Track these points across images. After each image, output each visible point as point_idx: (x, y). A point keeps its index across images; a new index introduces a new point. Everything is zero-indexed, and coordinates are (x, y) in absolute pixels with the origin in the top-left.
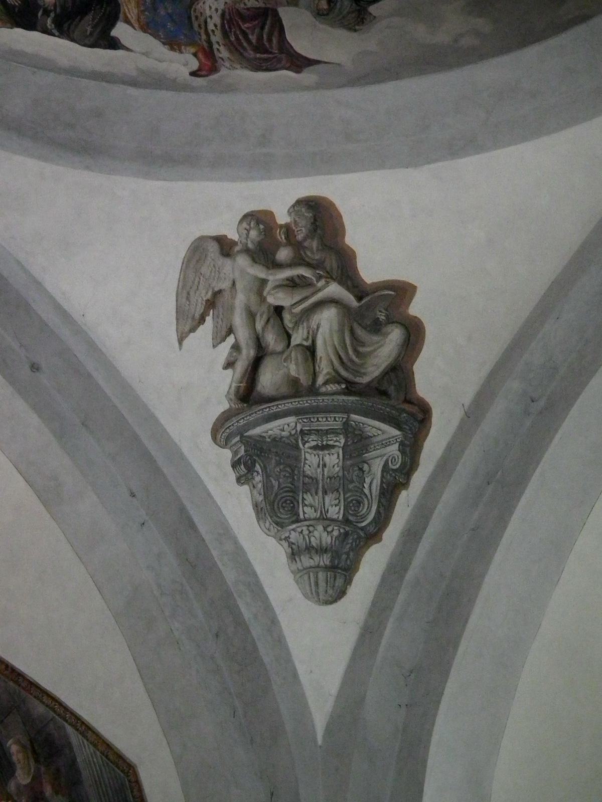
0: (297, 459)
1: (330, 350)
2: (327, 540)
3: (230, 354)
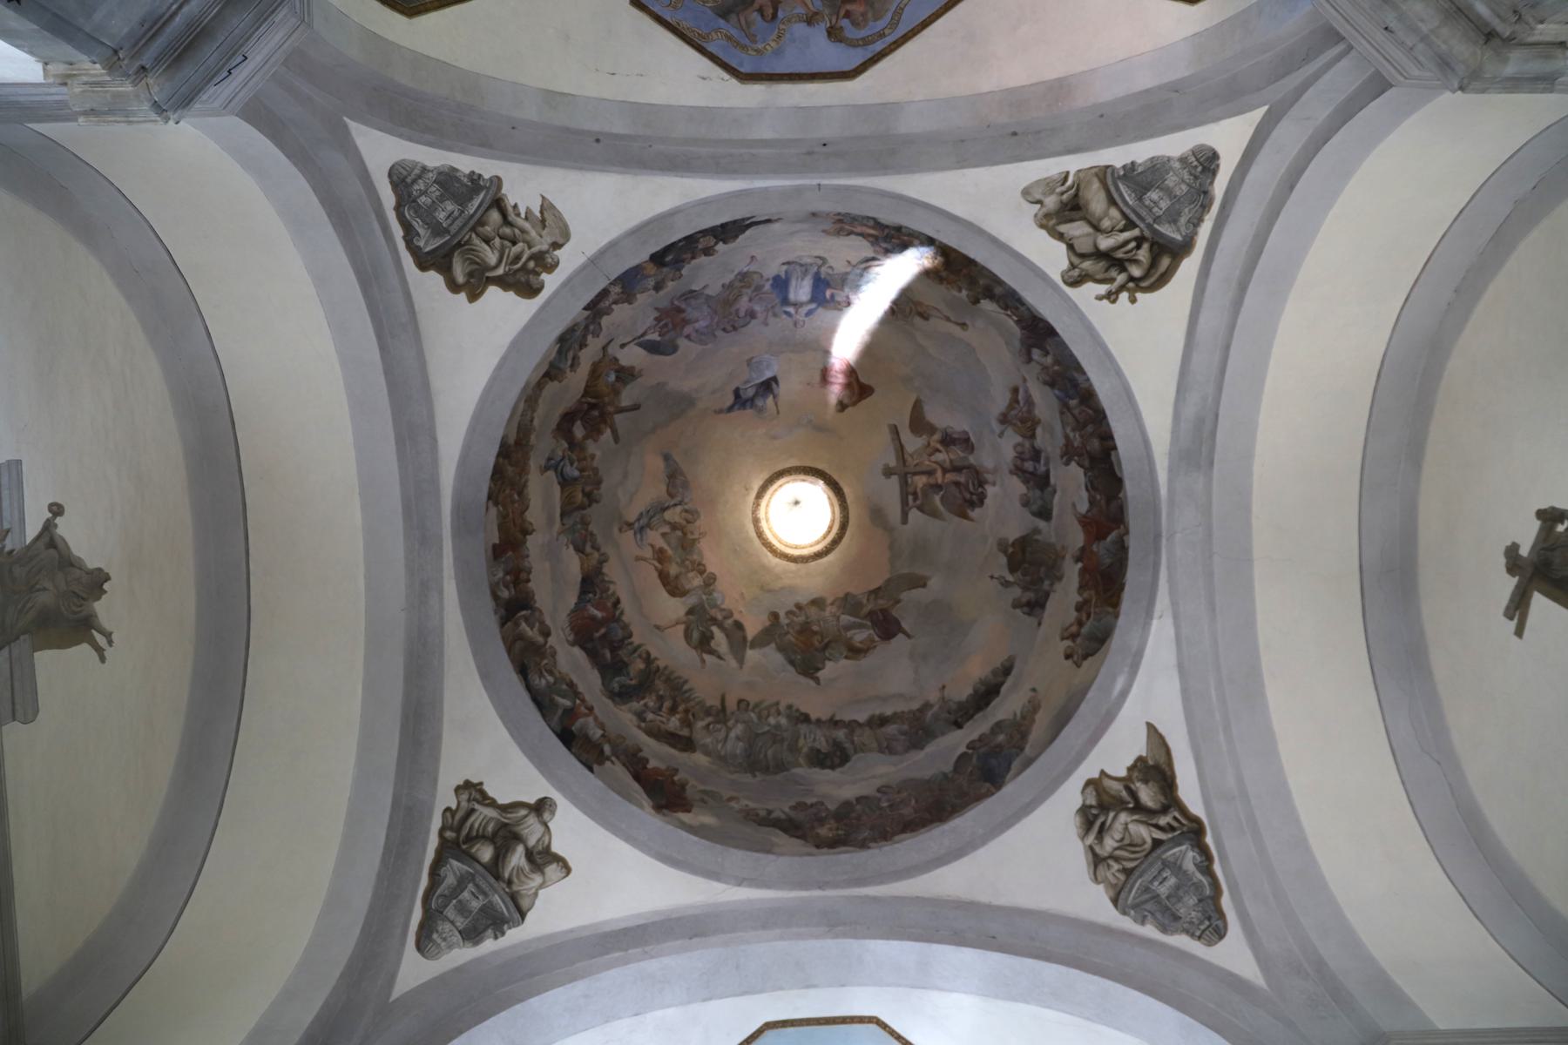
0: (456, 202)
1: (478, 248)
2: (416, 187)
3: (518, 210)
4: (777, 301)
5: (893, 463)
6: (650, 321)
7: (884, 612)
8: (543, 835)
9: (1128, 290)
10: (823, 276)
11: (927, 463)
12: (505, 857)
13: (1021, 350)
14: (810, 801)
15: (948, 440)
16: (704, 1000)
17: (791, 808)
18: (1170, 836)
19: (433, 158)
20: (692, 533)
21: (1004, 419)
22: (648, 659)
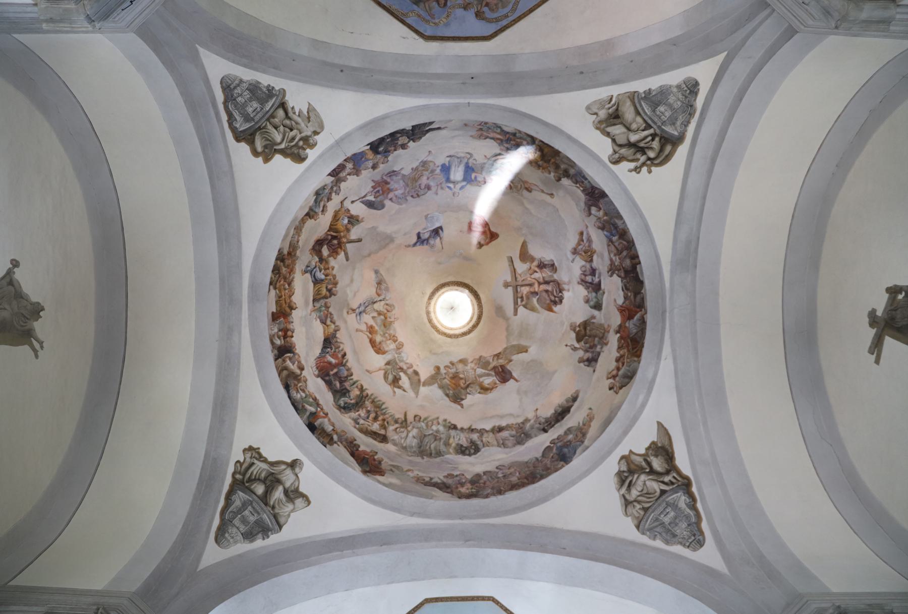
0: (258, 102)
2: (236, 91)
3: (295, 110)
4: (444, 180)
5: (509, 279)
6: (369, 188)
7: (502, 366)
8: (295, 481)
9: (647, 166)
10: (470, 165)
11: (529, 279)
12: (271, 492)
13: (584, 209)
14: (455, 473)
15: (542, 266)
16: (388, 583)
17: (444, 477)
18: (671, 487)
19: (247, 75)
20: (390, 318)
21: (575, 252)
22: (362, 389)
